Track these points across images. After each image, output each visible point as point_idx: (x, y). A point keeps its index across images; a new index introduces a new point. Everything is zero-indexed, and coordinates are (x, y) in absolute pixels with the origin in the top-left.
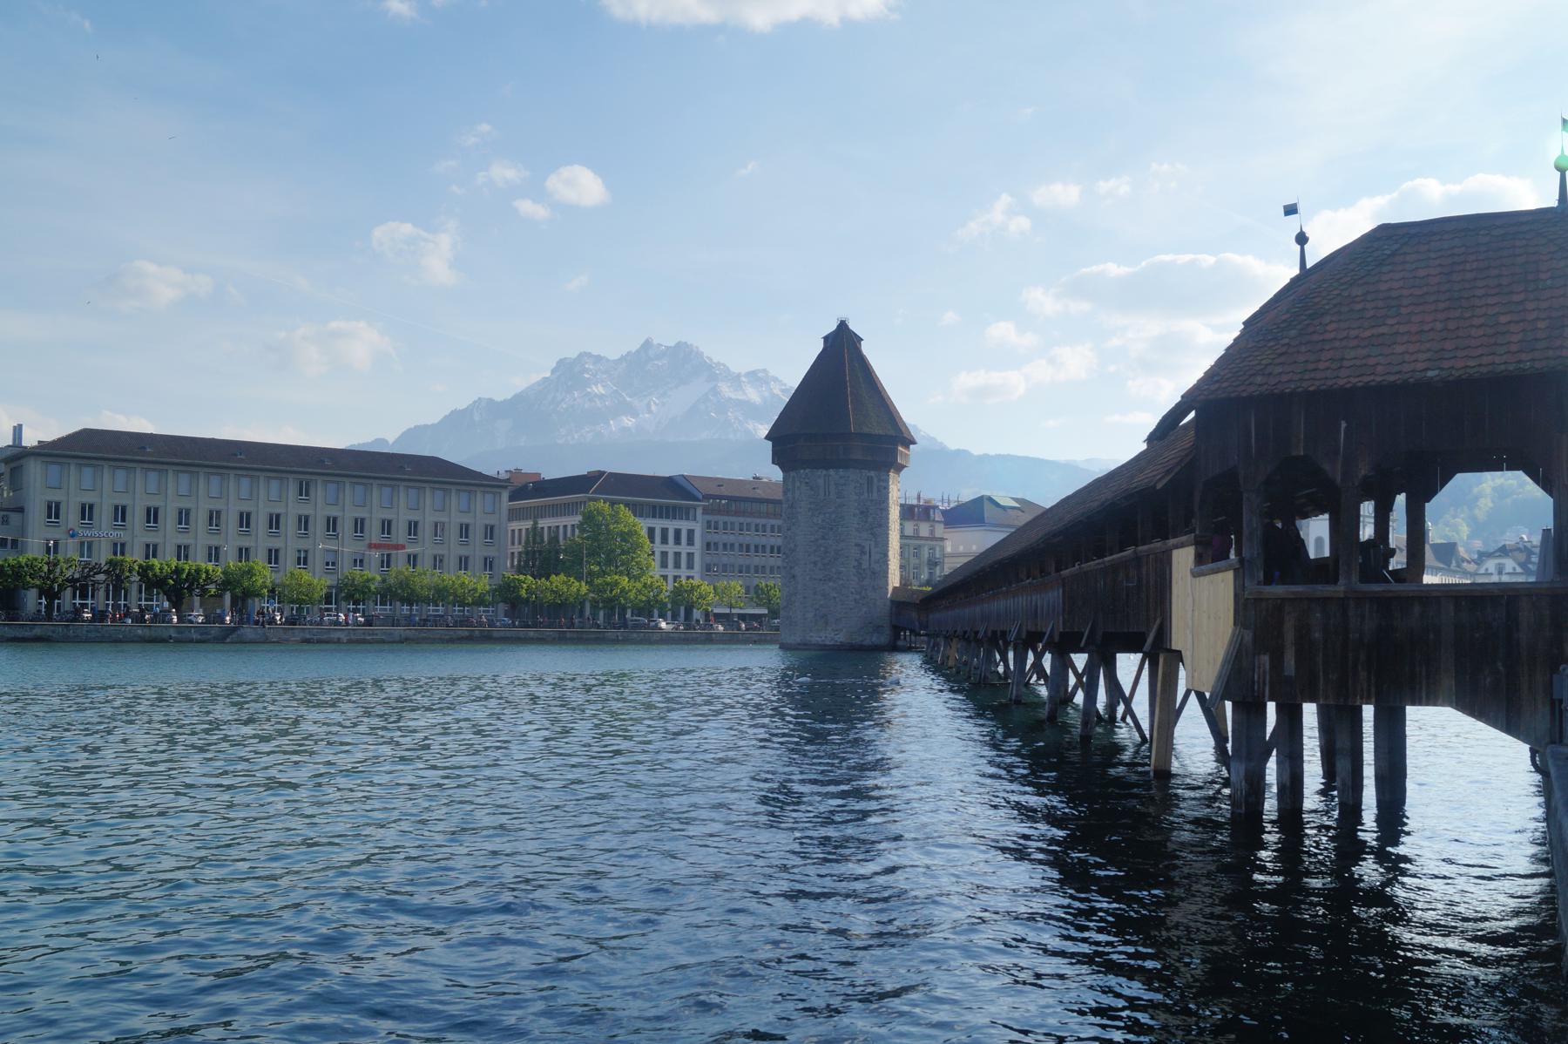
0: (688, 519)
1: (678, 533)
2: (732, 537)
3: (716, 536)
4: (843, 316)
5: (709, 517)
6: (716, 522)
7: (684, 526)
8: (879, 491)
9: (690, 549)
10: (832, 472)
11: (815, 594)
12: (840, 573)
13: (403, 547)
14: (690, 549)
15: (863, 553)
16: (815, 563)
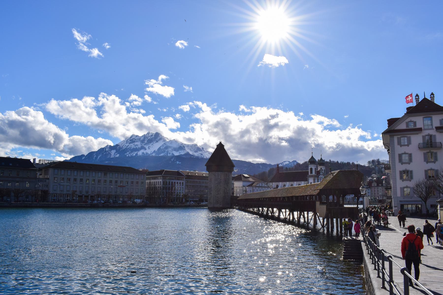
0: (182, 180)
1: (180, 183)
2: (191, 184)
3: (193, 184)
4: (221, 141)
5: (186, 180)
6: (191, 181)
7: (181, 182)
8: (228, 176)
9: (183, 187)
10: (219, 173)
11: (216, 197)
12: (221, 193)
13: (125, 186)
14: (183, 187)
15: (225, 189)
16: (216, 191)
